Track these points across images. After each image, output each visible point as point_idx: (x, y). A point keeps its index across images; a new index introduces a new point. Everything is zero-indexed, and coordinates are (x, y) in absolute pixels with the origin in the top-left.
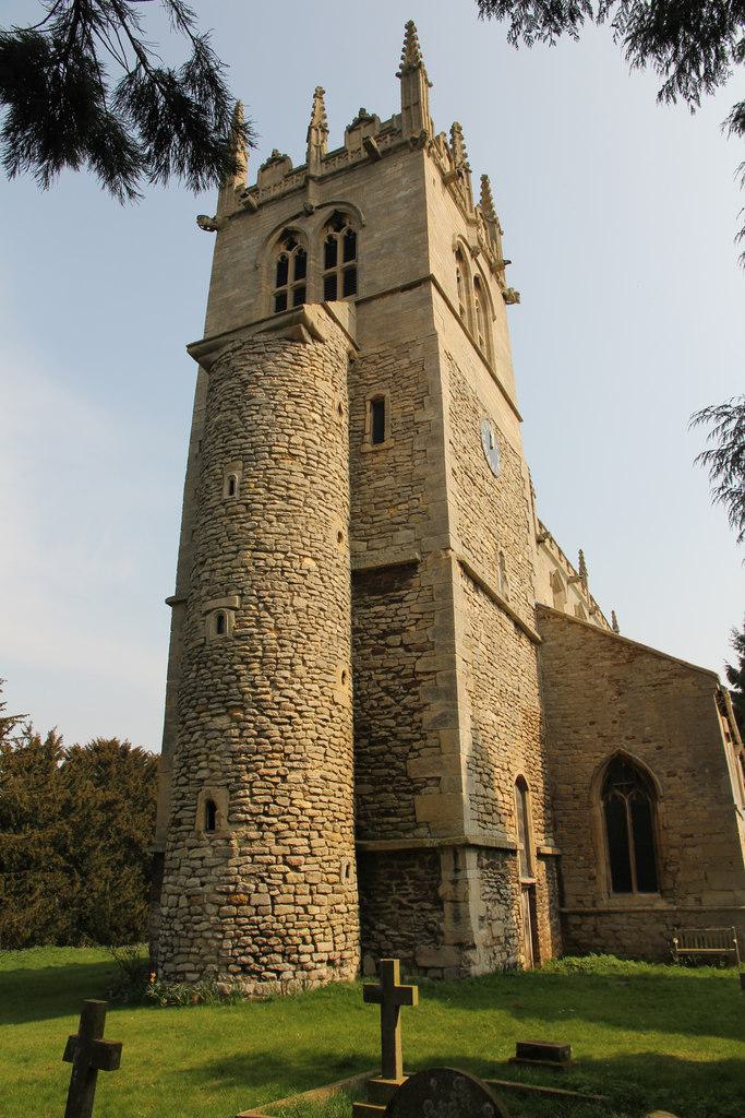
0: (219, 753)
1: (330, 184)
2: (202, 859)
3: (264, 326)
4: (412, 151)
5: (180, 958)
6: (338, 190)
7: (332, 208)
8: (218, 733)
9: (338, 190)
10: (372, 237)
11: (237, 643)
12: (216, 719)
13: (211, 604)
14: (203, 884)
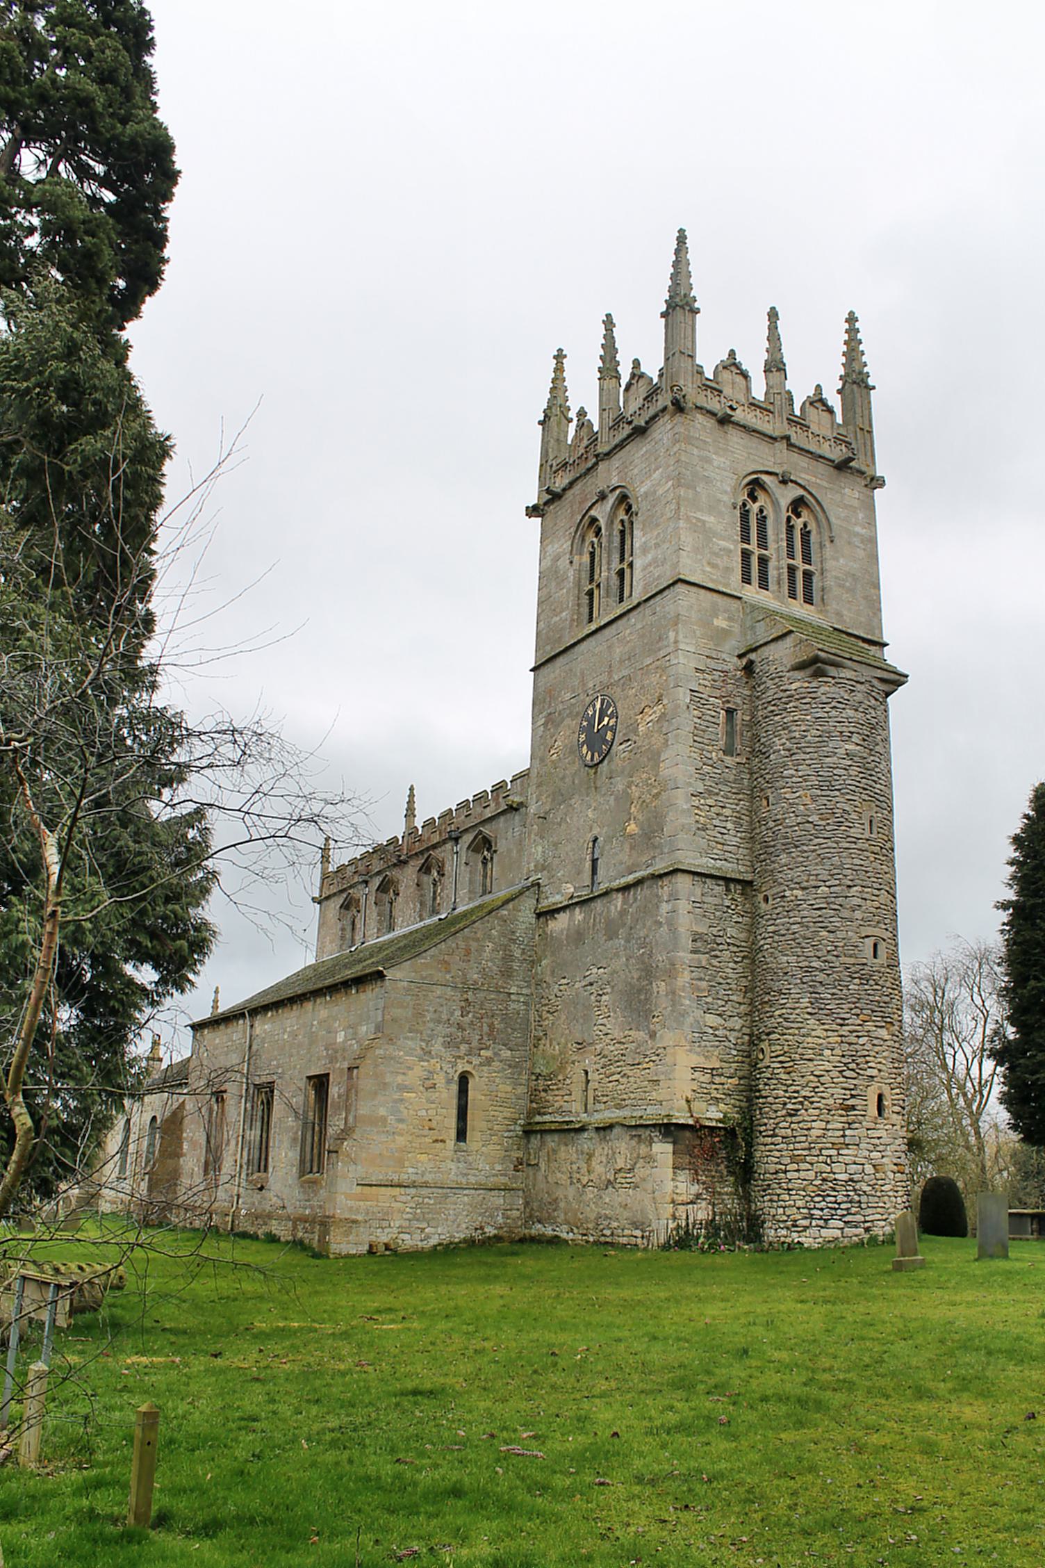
0: (884, 1058)
1: (795, 457)
2: (879, 1138)
3: (880, 674)
4: (866, 486)
5: (870, 1211)
6: (811, 476)
7: (801, 492)
8: (882, 1043)
9: (811, 476)
10: (837, 559)
11: (888, 970)
12: (879, 1030)
13: (869, 931)
14: (883, 1157)
